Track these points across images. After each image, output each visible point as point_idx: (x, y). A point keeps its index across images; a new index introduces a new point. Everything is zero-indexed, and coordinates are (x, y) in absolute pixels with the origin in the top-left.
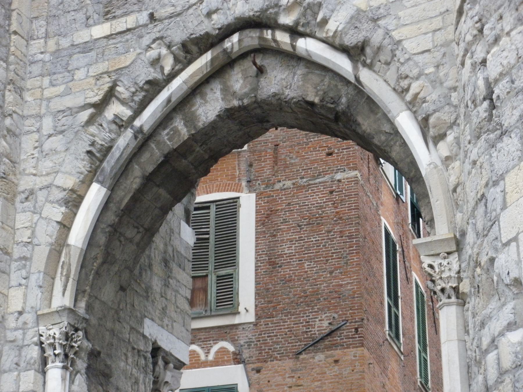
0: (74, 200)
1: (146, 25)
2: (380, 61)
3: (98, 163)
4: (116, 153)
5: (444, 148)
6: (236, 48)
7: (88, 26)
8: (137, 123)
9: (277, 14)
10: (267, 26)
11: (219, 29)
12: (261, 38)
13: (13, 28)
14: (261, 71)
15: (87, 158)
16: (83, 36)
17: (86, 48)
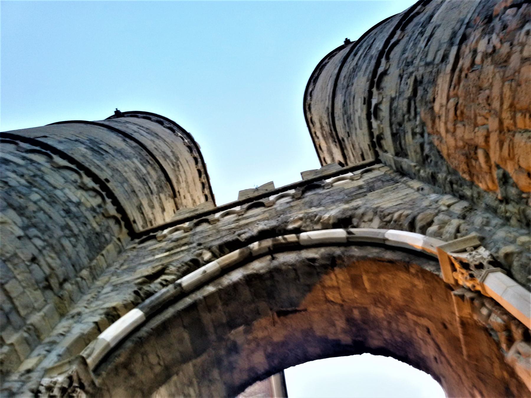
0: (112, 316)
1: (194, 248)
2: (364, 222)
3: (140, 301)
4: (157, 295)
5: (433, 229)
8: (179, 281)
9: (286, 226)
10: (278, 236)
11: (246, 239)
14: (273, 258)
15: (133, 294)
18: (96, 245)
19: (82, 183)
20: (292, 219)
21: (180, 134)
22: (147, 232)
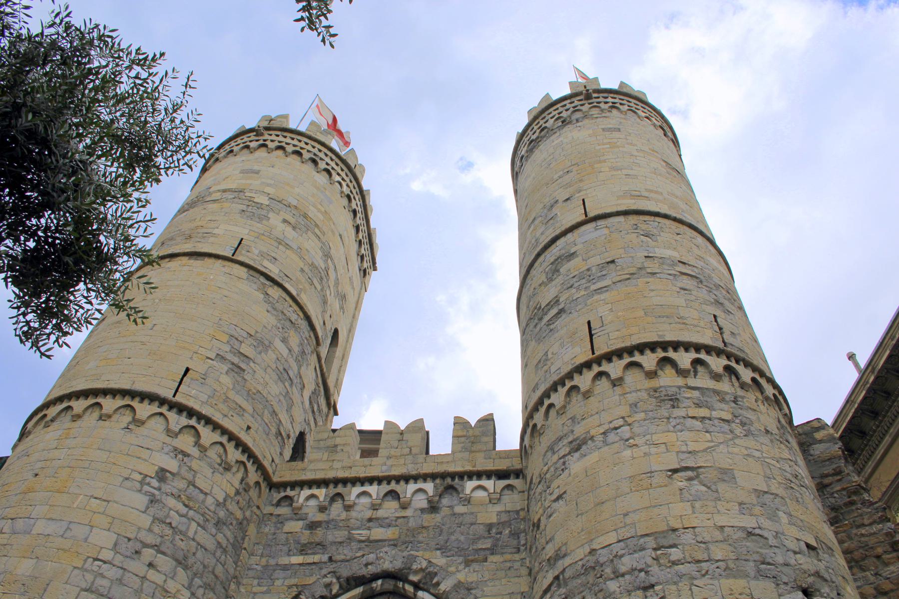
1: (325, 563)
6: (379, 588)
7: (289, 555)
9: (409, 574)
10: (400, 580)
12: (396, 586)
13: (245, 545)
16: (285, 560)
17: (285, 568)
18: (239, 539)
19: (226, 463)
20: (414, 567)
21: (338, 178)
22: (284, 485)
